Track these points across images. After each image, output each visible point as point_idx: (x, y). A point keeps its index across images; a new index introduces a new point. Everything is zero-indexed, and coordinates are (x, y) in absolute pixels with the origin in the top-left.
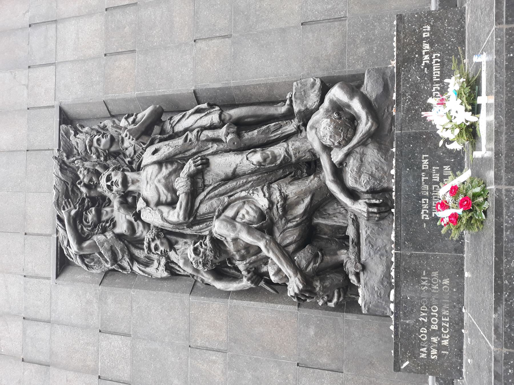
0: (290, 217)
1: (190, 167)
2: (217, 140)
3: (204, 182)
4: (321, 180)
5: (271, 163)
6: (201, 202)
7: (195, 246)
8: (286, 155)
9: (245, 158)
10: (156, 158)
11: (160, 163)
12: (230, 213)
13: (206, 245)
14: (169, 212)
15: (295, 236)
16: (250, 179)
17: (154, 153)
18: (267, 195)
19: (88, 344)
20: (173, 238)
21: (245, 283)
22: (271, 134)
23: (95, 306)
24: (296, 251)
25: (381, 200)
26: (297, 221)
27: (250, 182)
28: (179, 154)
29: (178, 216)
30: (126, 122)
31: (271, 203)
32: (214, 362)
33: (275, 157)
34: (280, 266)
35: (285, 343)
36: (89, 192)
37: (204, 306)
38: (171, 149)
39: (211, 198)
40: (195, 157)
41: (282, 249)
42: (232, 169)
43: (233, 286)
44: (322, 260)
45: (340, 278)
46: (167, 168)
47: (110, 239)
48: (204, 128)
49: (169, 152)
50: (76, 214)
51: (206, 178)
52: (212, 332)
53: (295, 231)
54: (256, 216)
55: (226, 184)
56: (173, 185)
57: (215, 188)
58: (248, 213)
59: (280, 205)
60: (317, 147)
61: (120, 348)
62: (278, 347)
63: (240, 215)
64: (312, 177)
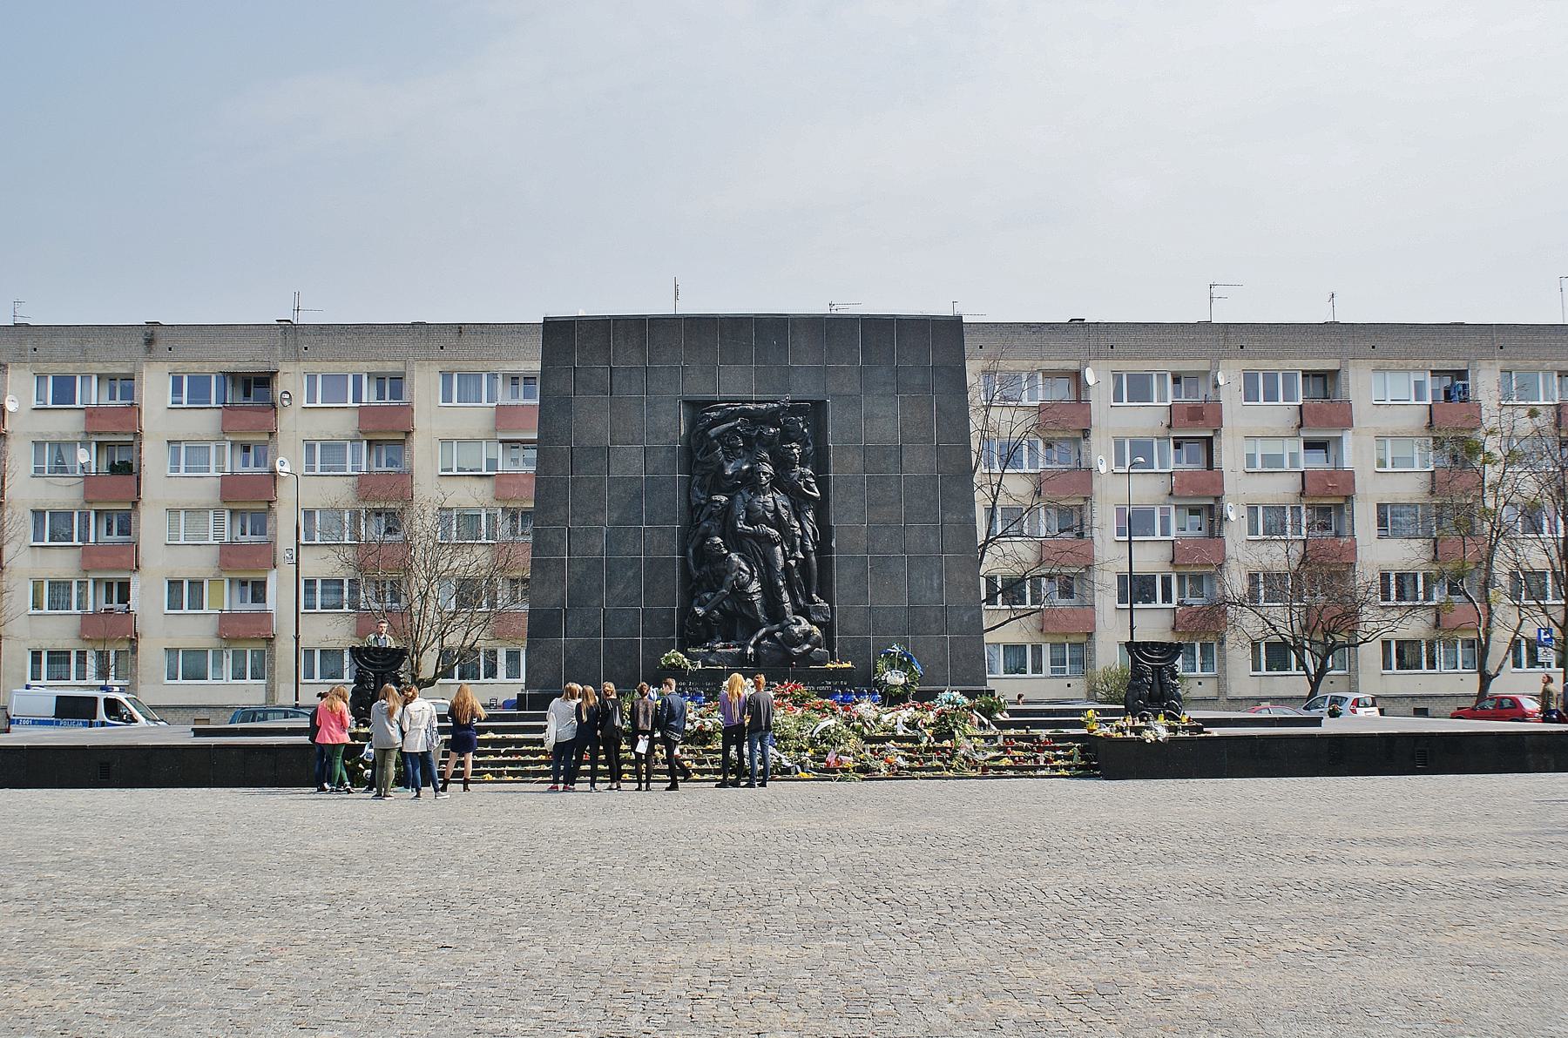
2: (793, 550)
6: (750, 543)
10: (780, 507)
11: (776, 510)
19: (632, 434)
24: (720, 611)
32: (634, 547)
38: (786, 519)
39: (751, 548)
41: (722, 602)
45: (704, 637)
52: (655, 544)
57: (759, 551)
60: (786, 622)
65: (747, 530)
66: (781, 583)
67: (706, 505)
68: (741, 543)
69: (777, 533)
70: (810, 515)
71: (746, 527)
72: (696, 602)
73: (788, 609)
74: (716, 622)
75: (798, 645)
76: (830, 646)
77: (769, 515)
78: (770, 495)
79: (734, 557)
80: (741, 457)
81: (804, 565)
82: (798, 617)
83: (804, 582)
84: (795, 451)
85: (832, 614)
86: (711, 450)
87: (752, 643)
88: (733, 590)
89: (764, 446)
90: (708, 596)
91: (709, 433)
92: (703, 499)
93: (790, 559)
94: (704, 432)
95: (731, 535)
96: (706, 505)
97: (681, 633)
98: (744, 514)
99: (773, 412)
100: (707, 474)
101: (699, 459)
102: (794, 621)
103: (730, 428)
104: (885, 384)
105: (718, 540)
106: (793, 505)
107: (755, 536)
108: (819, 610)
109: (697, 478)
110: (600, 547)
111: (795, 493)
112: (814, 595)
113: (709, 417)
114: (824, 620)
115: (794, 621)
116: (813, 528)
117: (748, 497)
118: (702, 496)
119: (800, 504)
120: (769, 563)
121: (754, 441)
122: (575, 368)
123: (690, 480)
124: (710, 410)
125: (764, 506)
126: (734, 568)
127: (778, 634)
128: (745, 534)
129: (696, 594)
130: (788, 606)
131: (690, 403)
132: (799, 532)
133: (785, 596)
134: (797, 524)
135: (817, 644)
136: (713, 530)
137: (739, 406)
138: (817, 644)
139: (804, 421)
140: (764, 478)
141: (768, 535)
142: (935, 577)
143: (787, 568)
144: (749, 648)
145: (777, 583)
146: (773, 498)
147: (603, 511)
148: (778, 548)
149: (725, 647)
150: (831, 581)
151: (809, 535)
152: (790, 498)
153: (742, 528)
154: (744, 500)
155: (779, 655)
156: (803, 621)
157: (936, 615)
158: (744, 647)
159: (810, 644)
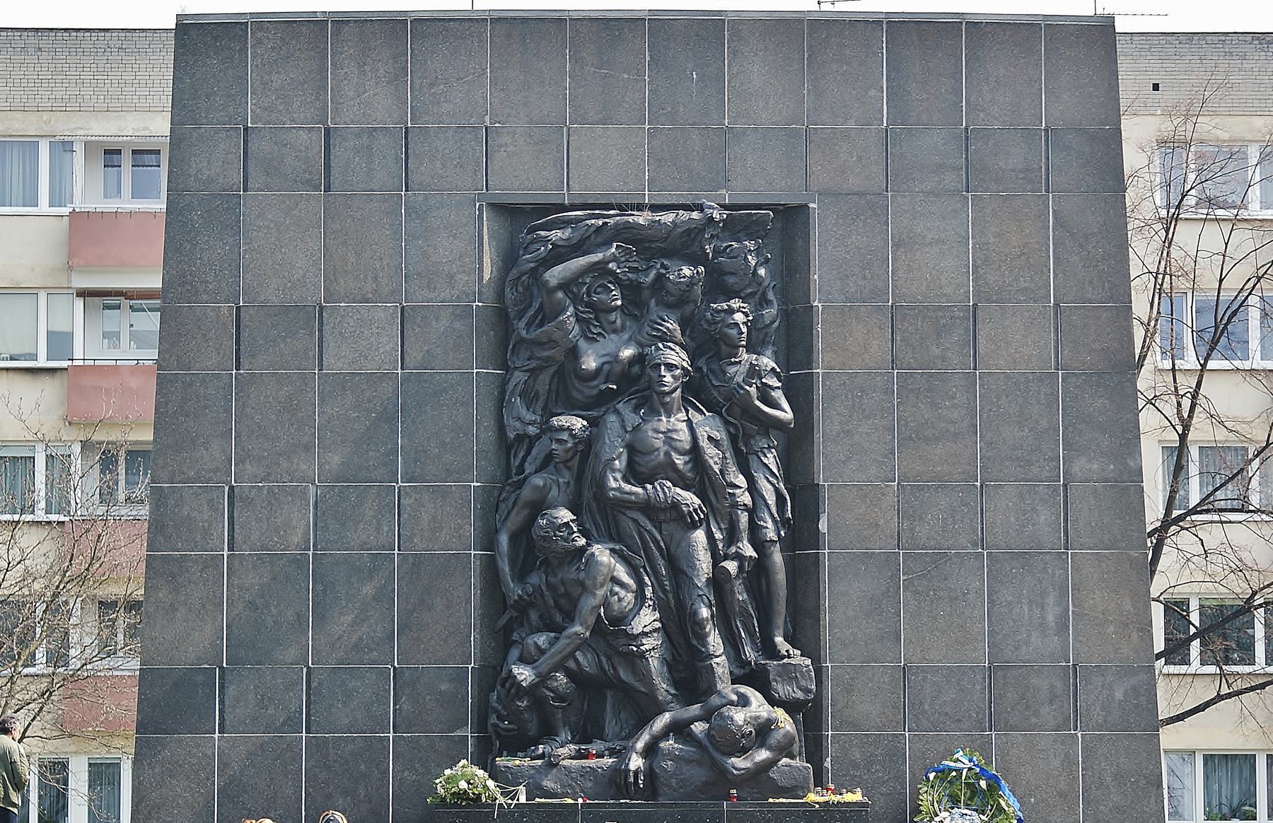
0: (616, 660)
1: (690, 499)
2: (732, 536)
3: (665, 521)
4: (668, 704)
5: (694, 632)
6: (635, 521)
7: (571, 523)
8: (704, 655)
9: (701, 593)
10: (704, 443)
11: (695, 451)
12: (622, 573)
13: (573, 540)
14: (619, 471)
15: (588, 669)
16: (670, 596)
17: (710, 438)
18: (646, 630)
19: (375, 279)
20: (575, 463)
21: (515, 591)
22: (740, 620)
23: (445, 294)
24: (569, 673)
25: (641, 786)
26: (609, 670)
27: (667, 597)
28: (709, 480)
29: (614, 489)
30: (766, 373)
31: (636, 637)
32: (378, 529)
33: (703, 638)
34: (549, 654)
35: (422, 646)
36: (648, 288)
37: (465, 510)
38: (716, 468)
40: (704, 509)
41: (572, 655)
42: (685, 568)
43: (505, 567)
44: (557, 707)
46: (686, 463)
47: (569, 339)
48: (752, 512)
49: (713, 465)
50: (612, 273)
51: (671, 523)
53: (595, 668)
54: (615, 613)
55: (663, 557)
56: (660, 474)
58: (620, 600)
59: (632, 649)
60: (715, 700)
61: (377, 349)
62: (416, 635)
63: (617, 589)
64: (673, 692)
65: (630, 493)
66: (705, 612)
67: (538, 437)
68: (617, 523)
69: (697, 501)
70: (771, 460)
71: (628, 487)
72: (515, 653)
73: (719, 671)
74: (560, 698)
75: (743, 751)
76: (814, 753)
77: (679, 461)
78: (682, 416)
79: (602, 554)
80: (615, 331)
81: (757, 572)
82: (744, 689)
83: (757, 609)
84: (739, 317)
85: (819, 682)
86: (548, 314)
87: (640, 745)
88: (597, 629)
89: (670, 306)
90: (542, 639)
91: (547, 275)
92: (532, 423)
93: (726, 557)
94: (535, 273)
95: (594, 505)
96: (538, 437)
97: (481, 723)
98: (624, 457)
99: (689, 231)
100: (540, 369)
101: (523, 333)
102: (735, 698)
103: (592, 267)
104: (940, 167)
105: (565, 515)
106: (733, 439)
107: (648, 508)
108: (790, 674)
109: (519, 377)
110: (300, 532)
111: (737, 411)
112: (779, 640)
113: (545, 241)
114: (800, 695)
115: (735, 698)
116: (777, 490)
117: (632, 419)
118: (529, 417)
119: (748, 437)
120: (679, 570)
121: (646, 293)
122: (246, 129)
123: (504, 382)
124: (548, 227)
125: (669, 440)
126: (600, 579)
127: (699, 728)
128: (623, 504)
129: (515, 636)
130: (721, 665)
131: (505, 210)
132: (746, 499)
133: (715, 641)
134: (741, 480)
135: (785, 749)
136: (554, 492)
137: (614, 218)
138: (785, 749)
139: (758, 252)
140: (668, 379)
141: (675, 506)
142: (1051, 599)
143: (719, 581)
144: (634, 756)
145: (695, 613)
146: (689, 422)
147: (308, 448)
148: (700, 536)
149: (580, 755)
150: (817, 608)
151: (767, 506)
152: (726, 423)
153: (619, 489)
154: (624, 427)
155: (698, 774)
156: (755, 697)
157: (1052, 687)
158: (621, 754)
159: (770, 749)
